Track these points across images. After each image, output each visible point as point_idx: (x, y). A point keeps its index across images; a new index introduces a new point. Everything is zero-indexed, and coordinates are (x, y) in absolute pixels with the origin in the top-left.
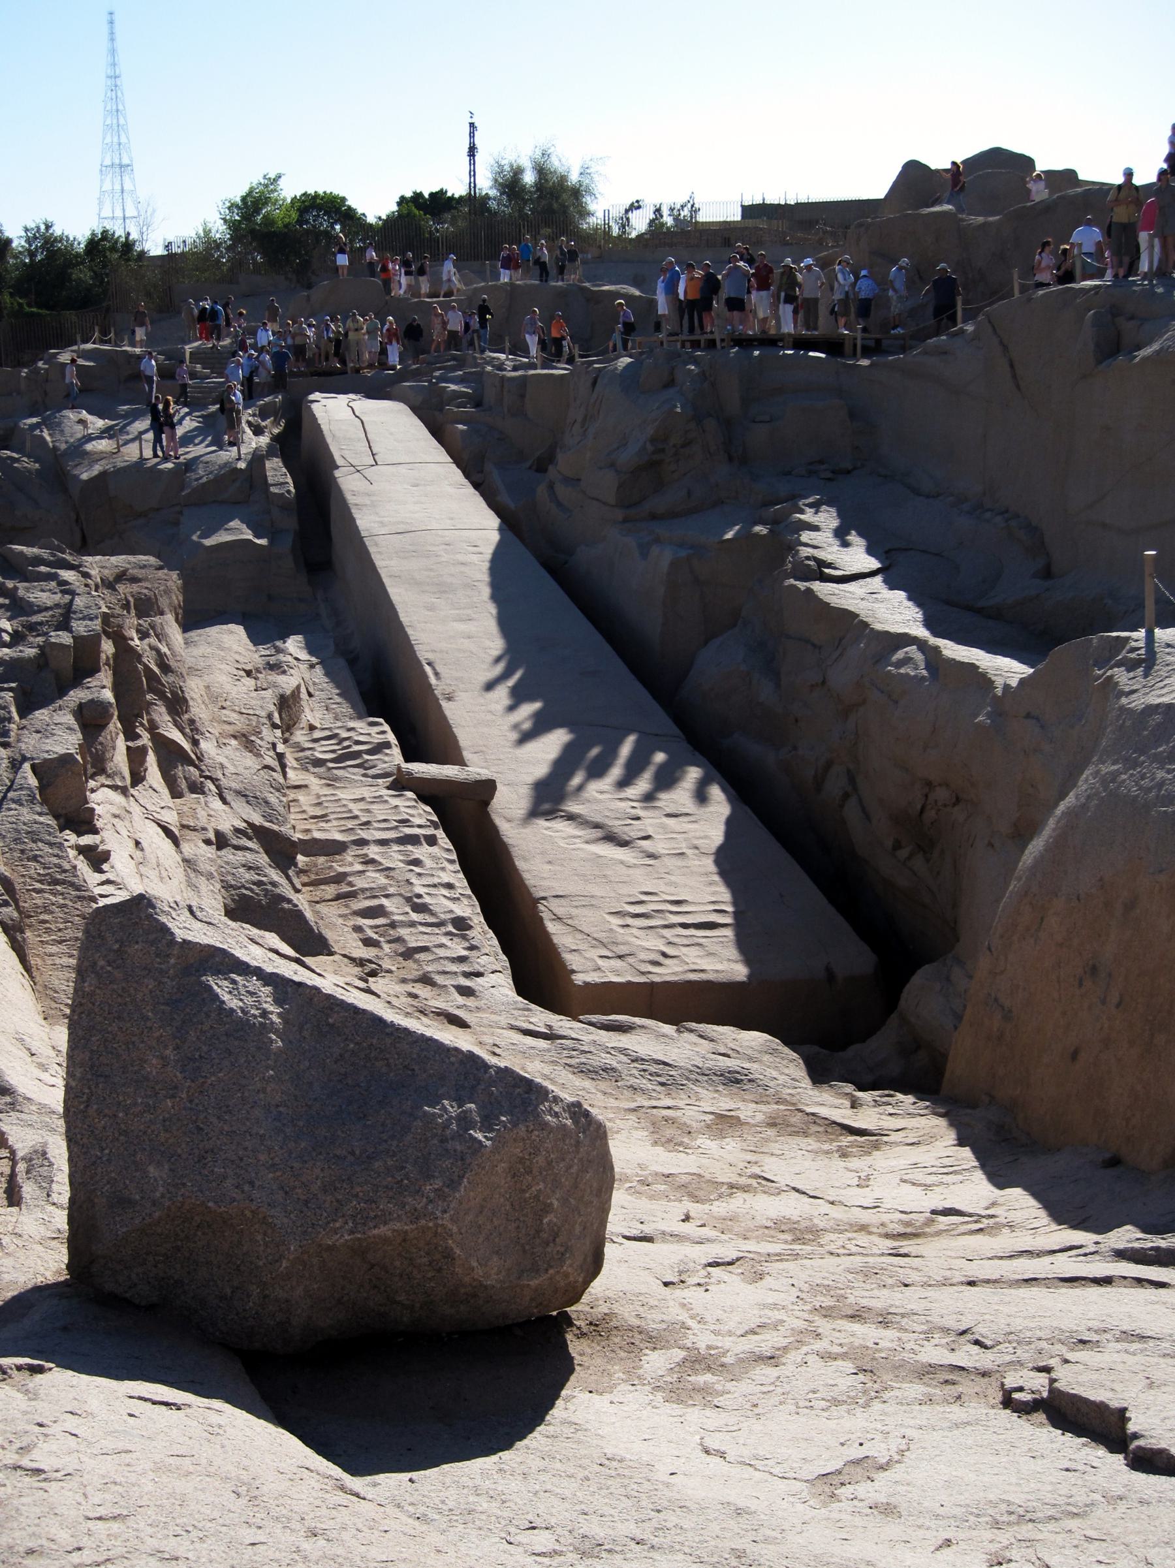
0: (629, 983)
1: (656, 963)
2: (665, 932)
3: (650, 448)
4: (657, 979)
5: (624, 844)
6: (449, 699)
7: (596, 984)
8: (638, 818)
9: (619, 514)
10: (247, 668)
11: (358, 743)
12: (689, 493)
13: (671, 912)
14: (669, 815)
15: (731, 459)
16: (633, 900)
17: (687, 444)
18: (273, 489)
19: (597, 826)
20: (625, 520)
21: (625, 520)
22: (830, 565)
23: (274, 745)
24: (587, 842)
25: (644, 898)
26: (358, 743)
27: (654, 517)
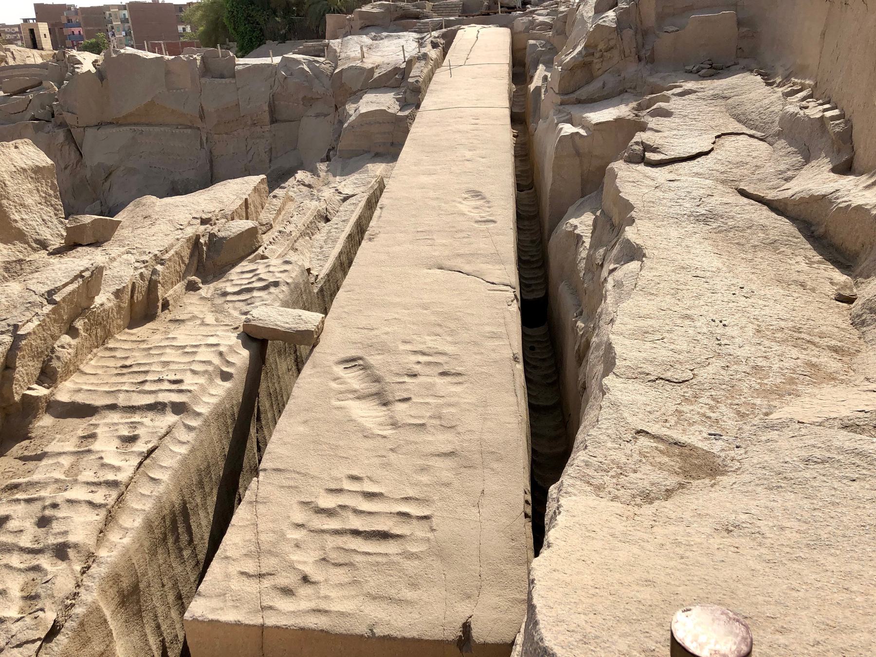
0: (238, 624)
1: (287, 592)
2: (332, 542)
3: (584, 53)
4: (271, 620)
5: (385, 405)
6: (370, 240)
7: (203, 622)
8: (415, 375)
9: (558, 99)
10: (205, 216)
11: (261, 280)
12: (604, 84)
13: (356, 512)
14: (444, 374)
15: (640, 59)
16: (333, 487)
17: (609, 50)
18: (410, 80)
19: (377, 380)
20: (561, 104)
21: (561, 104)
22: (655, 150)
23: (16, 327)
24: (358, 398)
25: (348, 485)
26: (261, 280)
27: (579, 102)
